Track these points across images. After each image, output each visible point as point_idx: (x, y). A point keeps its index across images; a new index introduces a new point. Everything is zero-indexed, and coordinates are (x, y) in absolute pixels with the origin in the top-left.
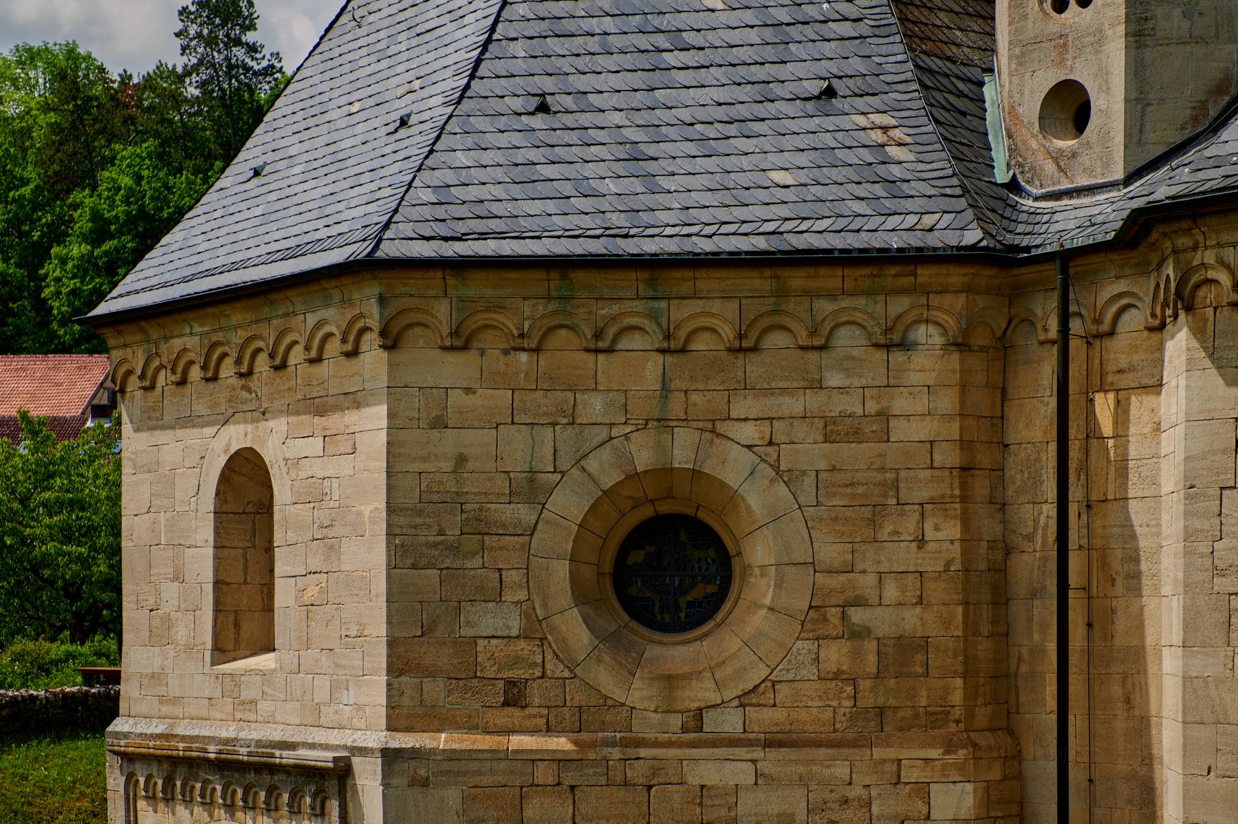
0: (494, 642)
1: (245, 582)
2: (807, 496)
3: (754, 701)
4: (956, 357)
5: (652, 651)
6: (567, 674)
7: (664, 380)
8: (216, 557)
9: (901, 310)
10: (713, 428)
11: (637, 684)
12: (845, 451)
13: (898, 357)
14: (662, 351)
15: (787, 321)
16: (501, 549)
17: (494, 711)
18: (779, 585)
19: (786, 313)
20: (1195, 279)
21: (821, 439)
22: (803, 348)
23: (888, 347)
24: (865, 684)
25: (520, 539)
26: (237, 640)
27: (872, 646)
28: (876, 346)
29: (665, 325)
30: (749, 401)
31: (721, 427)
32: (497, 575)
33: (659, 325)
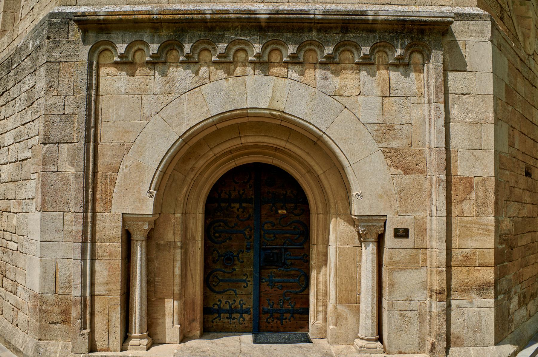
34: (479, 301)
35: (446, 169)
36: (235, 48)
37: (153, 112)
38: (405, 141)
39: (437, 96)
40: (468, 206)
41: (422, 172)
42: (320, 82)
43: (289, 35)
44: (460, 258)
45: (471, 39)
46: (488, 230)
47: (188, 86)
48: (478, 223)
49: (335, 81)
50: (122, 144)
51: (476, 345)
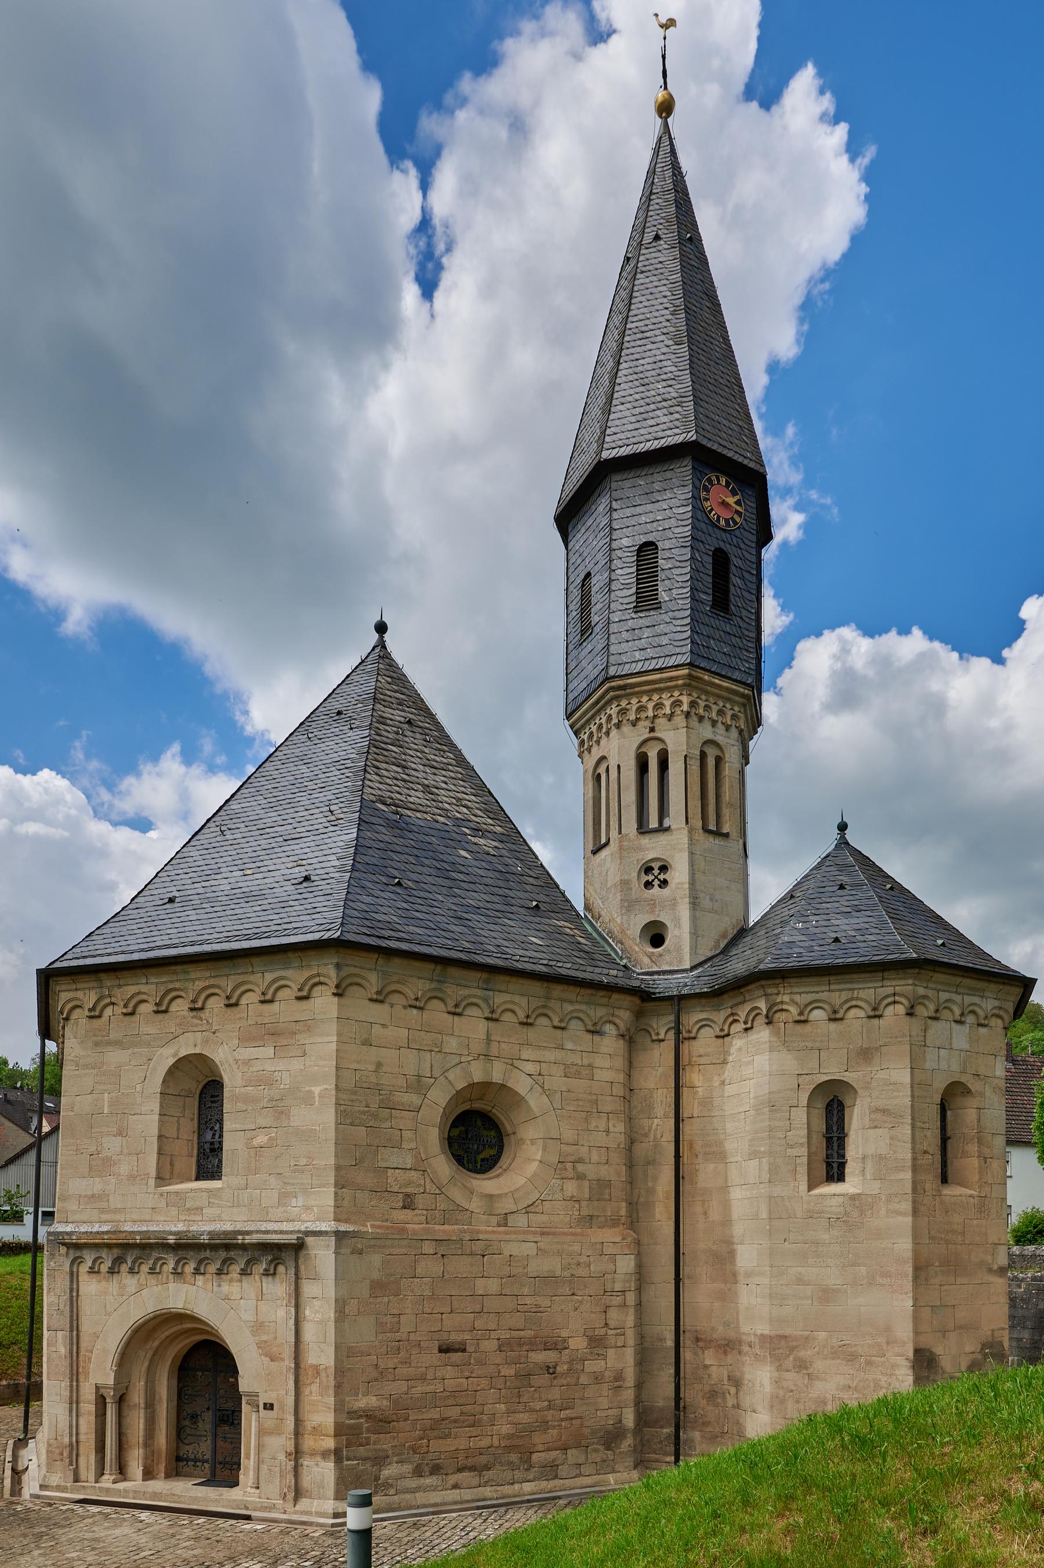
0: (397, 1171)
1: (178, 1138)
2: (557, 1105)
3: (533, 1211)
4: (621, 1042)
5: (475, 1182)
6: (437, 1191)
7: (488, 1034)
8: (160, 1121)
9: (602, 1014)
10: (512, 1063)
11: (474, 1199)
12: (574, 1082)
13: (597, 1038)
14: (487, 1019)
15: (550, 1014)
16: (401, 1118)
17: (397, 1211)
18: (544, 1150)
19: (550, 1008)
20: (775, 1009)
21: (563, 1075)
22: (555, 1027)
23: (592, 1032)
24: (584, 1204)
25: (412, 1113)
26: (172, 1173)
27: (586, 1183)
28: (588, 1031)
29: (492, 1005)
30: (529, 1051)
31: (516, 1063)
32: (399, 1133)
33: (488, 1004)
34: (322, 1464)
35: (295, 1358)
36: (160, 1262)
37: (113, 1310)
38: (272, 1336)
39: (289, 1302)
40: (315, 1388)
41: (283, 1360)
42: (216, 1289)
43: (192, 1253)
44: (310, 1429)
45: (320, 1252)
46: (329, 1408)
47: (134, 1290)
48: (322, 1402)
49: (225, 1288)
50: (95, 1333)
51: (320, 1498)
